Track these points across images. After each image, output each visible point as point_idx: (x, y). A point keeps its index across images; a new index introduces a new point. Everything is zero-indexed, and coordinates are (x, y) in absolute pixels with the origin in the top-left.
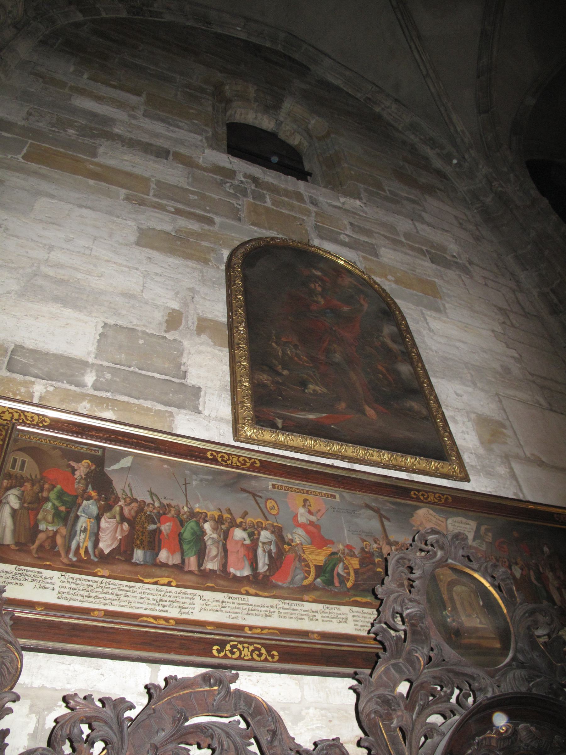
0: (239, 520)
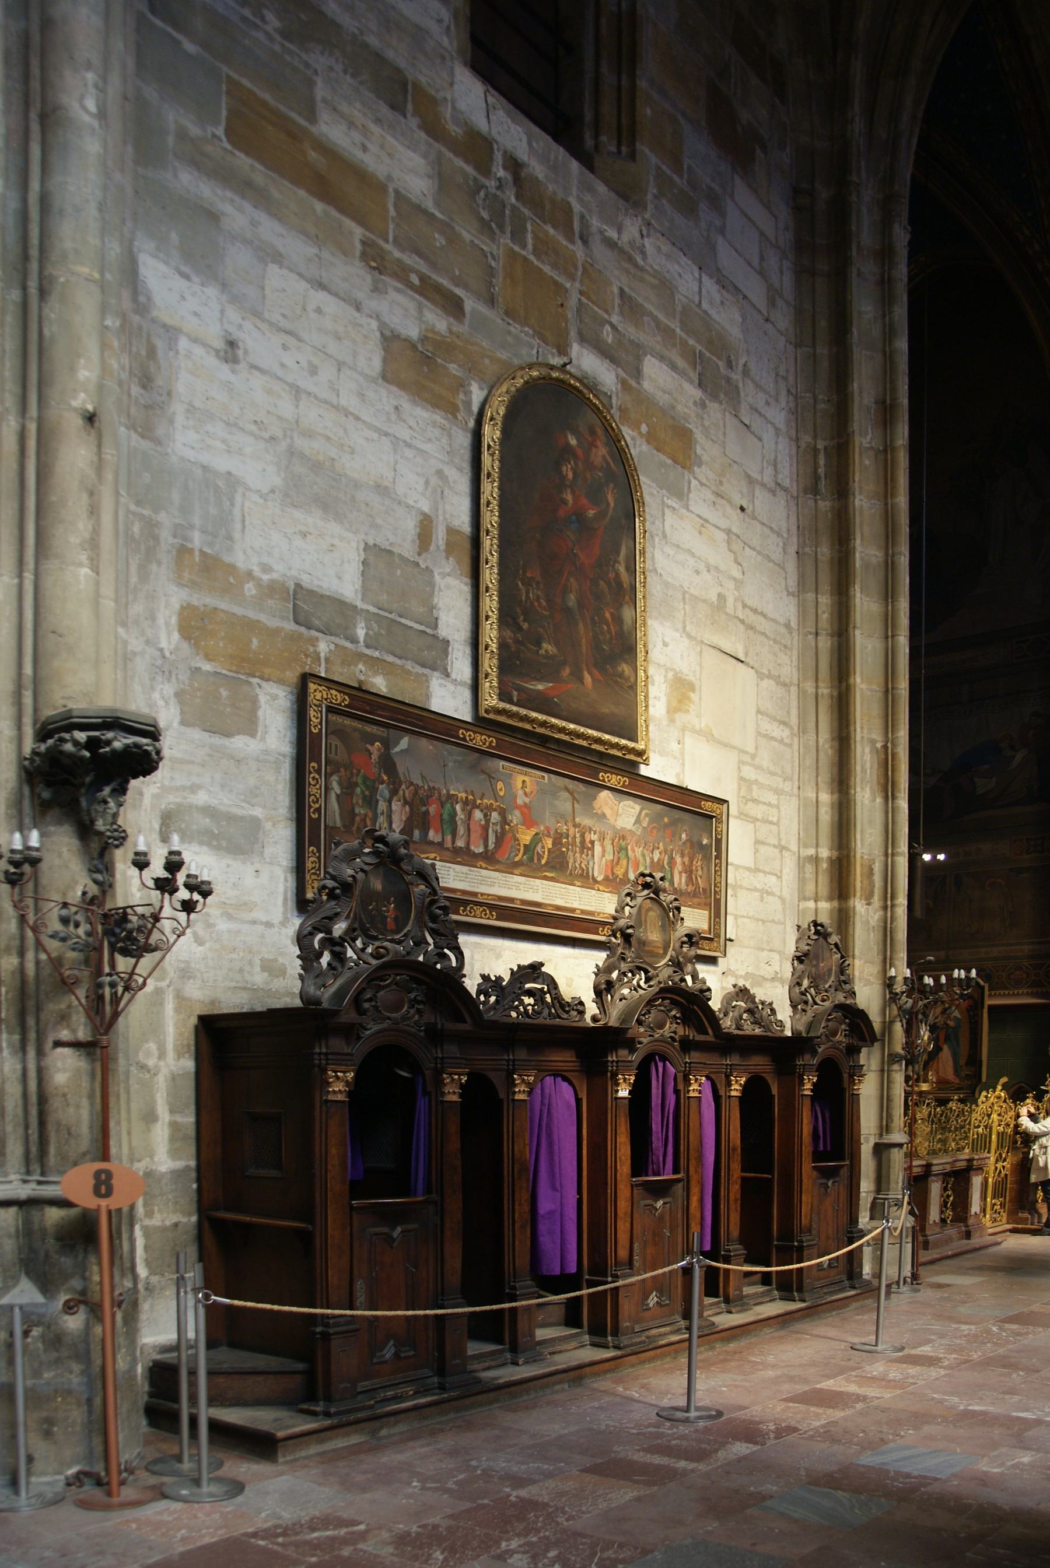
0: (479, 802)
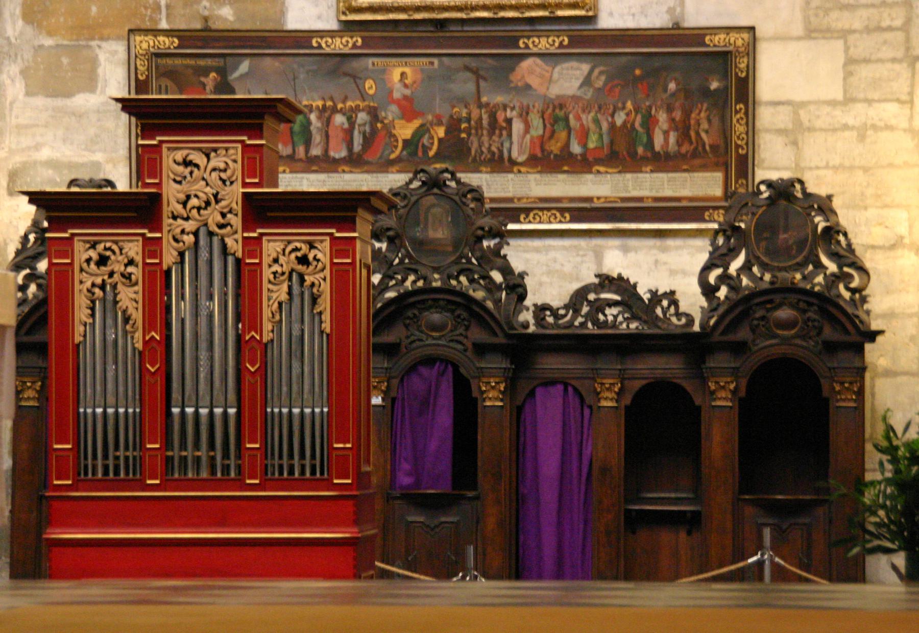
0: (340, 106)
